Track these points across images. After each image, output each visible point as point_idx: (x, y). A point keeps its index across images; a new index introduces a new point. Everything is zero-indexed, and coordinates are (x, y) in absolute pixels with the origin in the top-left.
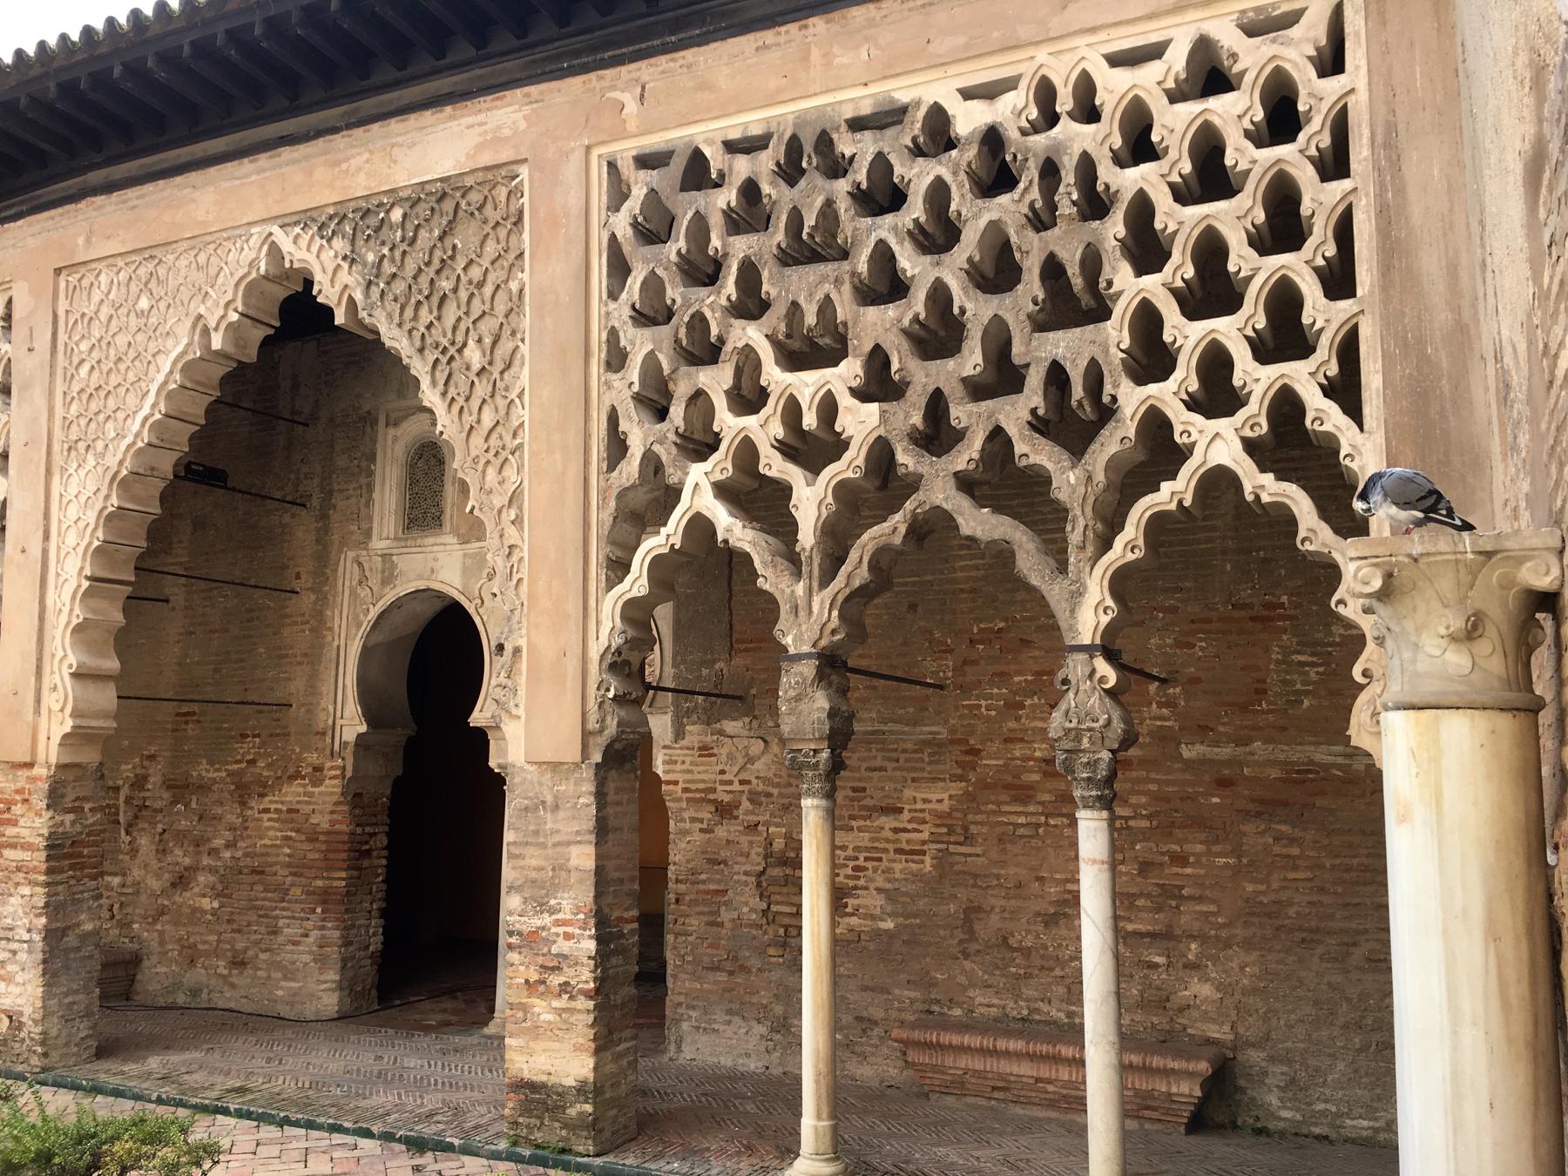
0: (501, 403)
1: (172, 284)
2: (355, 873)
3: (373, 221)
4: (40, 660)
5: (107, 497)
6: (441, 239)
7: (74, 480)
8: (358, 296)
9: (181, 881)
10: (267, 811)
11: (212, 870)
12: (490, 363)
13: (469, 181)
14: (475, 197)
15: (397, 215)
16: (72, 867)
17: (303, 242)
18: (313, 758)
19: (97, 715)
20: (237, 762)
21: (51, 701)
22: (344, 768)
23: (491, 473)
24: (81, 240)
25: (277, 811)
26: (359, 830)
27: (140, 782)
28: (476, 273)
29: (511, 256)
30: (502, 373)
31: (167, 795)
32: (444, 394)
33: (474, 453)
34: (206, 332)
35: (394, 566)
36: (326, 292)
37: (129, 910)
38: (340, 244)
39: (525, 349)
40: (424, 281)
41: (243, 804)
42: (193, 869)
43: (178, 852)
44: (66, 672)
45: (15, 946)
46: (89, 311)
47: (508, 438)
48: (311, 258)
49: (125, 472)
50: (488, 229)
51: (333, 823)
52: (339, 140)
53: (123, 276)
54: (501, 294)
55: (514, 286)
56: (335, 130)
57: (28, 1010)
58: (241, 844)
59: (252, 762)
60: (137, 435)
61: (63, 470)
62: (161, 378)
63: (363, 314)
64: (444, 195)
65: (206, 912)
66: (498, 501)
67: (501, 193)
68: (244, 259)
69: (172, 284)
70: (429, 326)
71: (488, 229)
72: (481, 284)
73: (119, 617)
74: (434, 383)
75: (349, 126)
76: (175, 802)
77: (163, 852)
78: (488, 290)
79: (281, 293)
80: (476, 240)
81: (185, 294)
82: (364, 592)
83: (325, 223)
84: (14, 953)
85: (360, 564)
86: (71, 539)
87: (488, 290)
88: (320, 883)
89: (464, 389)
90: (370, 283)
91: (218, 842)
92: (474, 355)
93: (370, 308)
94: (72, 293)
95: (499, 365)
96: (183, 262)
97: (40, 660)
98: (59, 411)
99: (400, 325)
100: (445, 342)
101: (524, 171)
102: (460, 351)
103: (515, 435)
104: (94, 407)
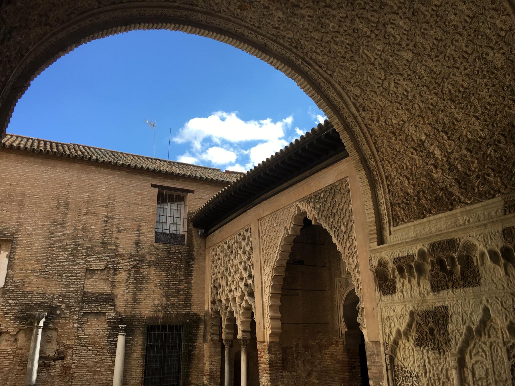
0: (351, 240)
1: (280, 219)
2: (351, 374)
3: (317, 198)
4: (263, 315)
5: (272, 273)
6: (332, 199)
7: (266, 269)
8: (317, 217)
9: (309, 375)
10: (326, 354)
11: (316, 371)
12: (347, 230)
13: (337, 184)
14: (338, 188)
15: (322, 195)
16: (276, 369)
17: (304, 205)
18: (335, 338)
19: (277, 328)
20: (318, 340)
21: (267, 325)
22: (343, 341)
23: (351, 259)
25: (329, 354)
26: (350, 360)
27: (297, 346)
28: (341, 207)
29: (348, 201)
30: (350, 232)
31: (303, 349)
32: (337, 239)
33: (346, 254)
34: (287, 230)
35: (348, 282)
36: (310, 217)
37: (298, 382)
38: (311, 204)
39: (354, 225)
40: (330, 210)
41: (321, 352)
42: (312, 371)
43: (308, 366)
44: (269, 318)
47: (353, 249)
48: (306, 209)
50: (342, 195)
51: (343, 358)
52: (308, 179)
53: (270, 219)
54: (347, 212)
55: (350, 209)
56: (307, 177)
58: (322, 364)
59: (321, 340)
60: (277, 257)
61: (264, 267)
62: (280, 243)
63: (318, 221)
64: (332, 188)
65: (315, 384)
66: (353, 267)
67: (344, 185)
68: (292, 211)
69: (280, 219)
70: (332, 222)
71: (342, 195)
72: (342, 210)
73: (279, 303)
74: (335, 237)
75: (310, 175)
76: (306, 351)
77: (304, 366)
78: (344, 210)
79: (303, 218)
80: (340, 198)
81: (282, 222)
82: (342, 290)
83: (307, 200)
85: (340, 282)
86: (267, 284)
87: (344, 210)
88: (342, 376)
89: (342, 237)
90: (318, 213)
91: (316, 363)
92: (343, 228)
93: (319, 219)
94: (262, 224)
95: (349, 230)
96: (281, 214)
97: (263, 315)
98: (262, 253)
99: (326, 223)
100: (336, 226)
101: (348, 179)
102: (340, 227)
103: (355, 249)
104: (268, 251)
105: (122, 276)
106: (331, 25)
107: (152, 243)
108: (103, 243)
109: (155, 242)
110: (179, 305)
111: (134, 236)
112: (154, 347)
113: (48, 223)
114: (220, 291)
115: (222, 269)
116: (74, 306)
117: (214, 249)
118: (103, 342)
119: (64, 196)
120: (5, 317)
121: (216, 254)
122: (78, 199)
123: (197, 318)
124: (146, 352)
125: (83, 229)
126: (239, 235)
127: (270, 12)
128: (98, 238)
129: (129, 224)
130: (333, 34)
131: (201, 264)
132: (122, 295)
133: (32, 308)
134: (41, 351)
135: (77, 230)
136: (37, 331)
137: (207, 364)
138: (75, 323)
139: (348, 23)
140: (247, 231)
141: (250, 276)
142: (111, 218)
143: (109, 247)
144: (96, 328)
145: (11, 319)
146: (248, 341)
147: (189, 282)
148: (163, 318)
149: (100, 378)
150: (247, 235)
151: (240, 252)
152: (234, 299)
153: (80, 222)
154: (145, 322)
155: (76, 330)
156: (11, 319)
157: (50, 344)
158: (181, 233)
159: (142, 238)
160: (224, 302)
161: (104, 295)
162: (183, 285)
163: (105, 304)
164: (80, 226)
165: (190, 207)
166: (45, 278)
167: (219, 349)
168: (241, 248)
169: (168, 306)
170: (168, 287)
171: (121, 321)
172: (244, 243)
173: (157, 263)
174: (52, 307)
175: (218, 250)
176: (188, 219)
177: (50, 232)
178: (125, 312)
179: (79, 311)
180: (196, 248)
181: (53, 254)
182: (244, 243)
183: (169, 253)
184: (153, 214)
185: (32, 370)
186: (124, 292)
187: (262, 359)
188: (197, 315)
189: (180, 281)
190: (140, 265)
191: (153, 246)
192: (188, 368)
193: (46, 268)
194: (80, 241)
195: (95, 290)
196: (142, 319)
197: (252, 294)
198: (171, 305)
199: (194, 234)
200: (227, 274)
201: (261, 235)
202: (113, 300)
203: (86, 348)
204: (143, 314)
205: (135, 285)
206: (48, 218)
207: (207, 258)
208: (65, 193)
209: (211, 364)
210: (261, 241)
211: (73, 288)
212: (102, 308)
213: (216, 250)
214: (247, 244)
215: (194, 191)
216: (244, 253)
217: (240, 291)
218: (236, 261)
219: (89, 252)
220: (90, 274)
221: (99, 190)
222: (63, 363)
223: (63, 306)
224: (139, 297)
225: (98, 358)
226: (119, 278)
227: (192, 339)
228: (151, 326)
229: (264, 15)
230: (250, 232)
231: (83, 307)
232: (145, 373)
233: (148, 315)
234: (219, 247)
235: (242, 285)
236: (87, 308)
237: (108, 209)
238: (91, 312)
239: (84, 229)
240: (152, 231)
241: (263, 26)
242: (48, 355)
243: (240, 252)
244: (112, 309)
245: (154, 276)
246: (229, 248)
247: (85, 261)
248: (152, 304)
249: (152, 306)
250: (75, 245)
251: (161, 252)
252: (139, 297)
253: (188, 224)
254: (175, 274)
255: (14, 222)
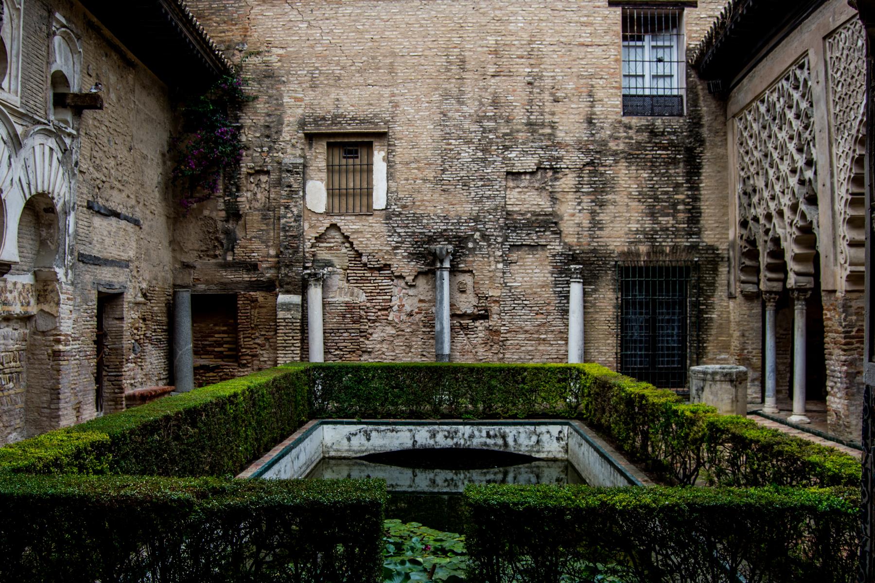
24: (831, 19)
45: (836, 380)
46: (838, 55)
49: (860, 136)
57: (842, 411)
84: (835, 383)
98: (832, 111)
104: (845, 105)
105: (568, 181)
107: (619, 118)
108: (530, 124)
109: (624, 115)
110: (678, 230)
111: (583, 107)
112: (634, 303)
113: (436, 97)
114: (755, 199)
115: (757, 155)
116: (493, 235)
117: (741, 119)
118: (548, 294)
119: (455, 48)
120: (396, 254)
121: (746, 128)
122: (479, 49)
123: (713, 253)
124: (622, 312)
125: (493, 102)
126: (787, 79)
128: (520, 117)
129: (571, 86)
131: (719, 150)
132: (573, 216)
133: (431, 240)
134: (452, 305)
135: (484, 105)
136: (442, 275)
137: (737, 334)
138: (498, 262)
140: (801, 67)
141: (810, 163)
142: (541, 78)
143: (541, 131)
144: (533, 273)
145: (404, 257)
146: (810, 292)
147: (694, 187)
148: (648, 254)
149: (546, 351)
150: (802, 75)
151: (790, 115)
152: (781, 213)
153: (486, 91)
154: (616, 262)
155: (501, 275)
156: (404, 257)
157: (464, 295)
158: (675, 92)
159: (598, 109)
160: (762, 221)
161: (540, 215)
162: (682, 194)
163: (544, 231)
164: (487, 98)
165: (690, 38)
166: (443, 190)
167: (757, 310)
168: (790, 107)
169: (656, 232)
170: (656, 199)
171: (574, 259)
172: (796, 95)
173: (630, 154)
174: (460, 237)
175: (749, 118)
176: (688, 62)
177: (441, 113)
178: (579, 244)
179: (502, 244)
180: (706, 120)
181: (451, 150)
182: (796, 95)
183: (653, 132)
184: (616, 61)
185: (442, 331)
186: (575, 209)
187: (829, 323)
188: (712, 248)
189: (677, 186)
190: (599, 159)
191: (620, 122)
192: (699, 342)
193: (443, 174)
194: (492, 124)
195: (524, 208)
196: (610, 257)
197: (812, 200)
198: (661, 230)
199: (701, 93)
200: (767, 166)
201: (830, 72)
202: (556, 223)
203: (520, 302)
204: (611, 248)
205: (593, 197)
206: (436, 89)
207: (730, 137)
208: (457, 40)
209: (743, 336)
210: (831, 84)
211: (488, 204)
212: (538, 237)
213: (746, 119)
214: (803, 96)
215: (696, 3)
216: (798, 116)
217: (790, 195)
218: (782, 136)
219: (508, 143)
220: (513, 180)
221: (512, 27)
222: (487, 325)
223: (477, 235)
224: (601, 217)
225: (540, 319)
226: (564, 186)
227: (705, 290)
228: (627, 268)
230: (809, 69)
231: (508, 237)
232: (621, 346)
233: (621, 249)
234: (750, 112)
235: (793, 181)
236: (514, 238)
237: (532, 62)
238: (522, 245)
239: (495, 103)
240: (616, 95)
242: (464, 311)
243: (790, 115)
244: (555, 239)
245: (627, 179)
246: (768, 111)
247: (504, 158)
248: (627, 229)
249: (627, 234)
250: (483, 132)
251: (637, 132)
252: (601, 217)
253: (687, 73)
254: (667, 172)
255: (386, 104)
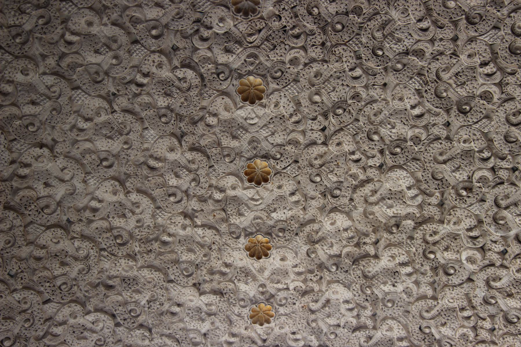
106: (464, 256)
127: (323, 300)
130: (483, 276)
139: (497, 235)
229: (313, 312)
241: (329, 339)
